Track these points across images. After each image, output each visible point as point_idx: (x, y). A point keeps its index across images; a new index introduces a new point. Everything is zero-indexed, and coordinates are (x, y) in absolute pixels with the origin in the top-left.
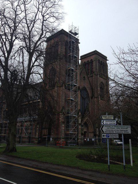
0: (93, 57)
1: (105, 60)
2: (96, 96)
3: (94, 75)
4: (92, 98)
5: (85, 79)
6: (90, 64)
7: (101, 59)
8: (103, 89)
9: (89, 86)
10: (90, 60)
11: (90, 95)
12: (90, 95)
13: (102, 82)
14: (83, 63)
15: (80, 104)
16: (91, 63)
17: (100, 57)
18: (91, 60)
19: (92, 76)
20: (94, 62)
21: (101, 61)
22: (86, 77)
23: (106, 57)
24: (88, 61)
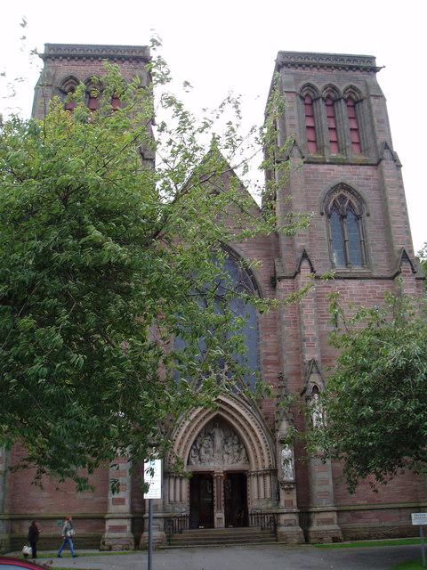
8: (358, 218)
13: (343, 186)
21: (334, 89)
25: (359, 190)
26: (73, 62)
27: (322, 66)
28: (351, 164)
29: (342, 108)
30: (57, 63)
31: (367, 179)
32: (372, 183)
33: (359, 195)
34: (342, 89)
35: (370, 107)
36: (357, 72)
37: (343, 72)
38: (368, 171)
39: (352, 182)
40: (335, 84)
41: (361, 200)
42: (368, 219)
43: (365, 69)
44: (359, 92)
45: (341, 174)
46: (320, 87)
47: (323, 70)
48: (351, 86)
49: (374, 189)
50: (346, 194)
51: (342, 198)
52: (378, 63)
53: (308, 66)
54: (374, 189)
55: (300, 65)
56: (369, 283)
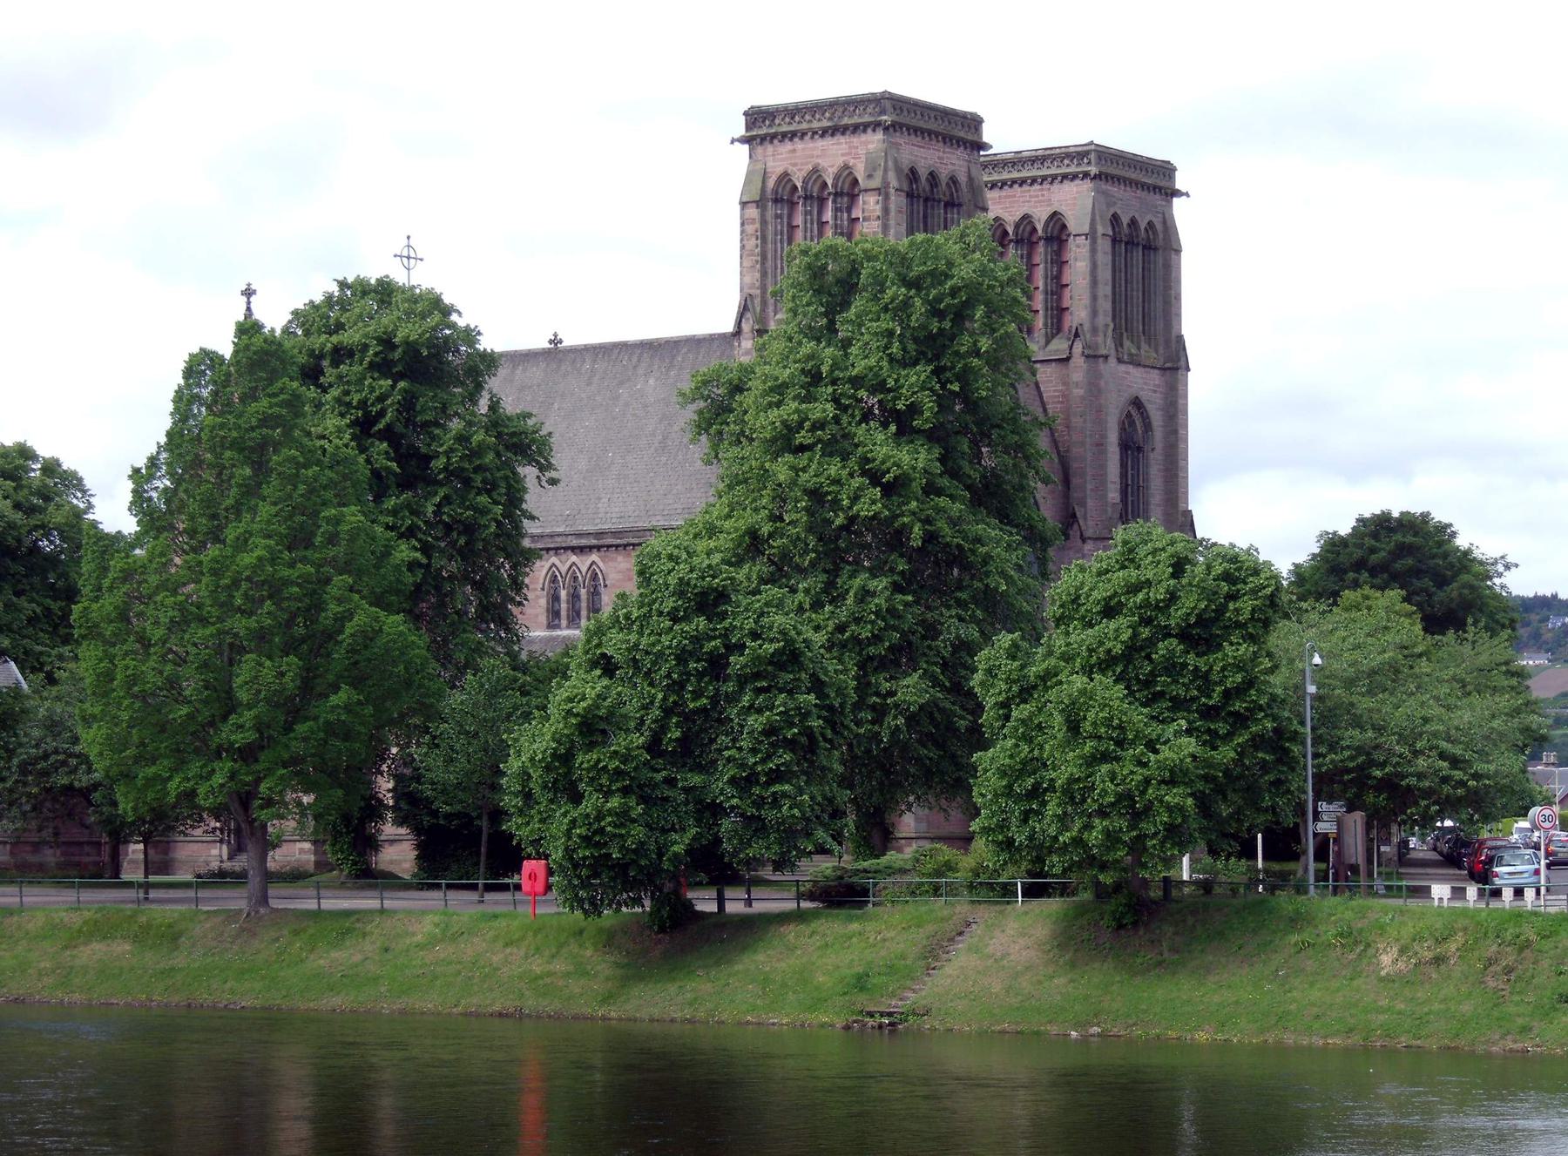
1: (1157, 199)
7: (1129, 204)
8: (1139, 449)
10: (1041, 215)
13: (1137, 403)
18: (1055, 213)
21: (1133, 223)
23: (1165, 170)
24: (1026, 218)
25: (1149, 407)
26: (913, 137)
28: (1145, 366)
29: (1138, 254)
31: (1155, 392)
33: (1148, 417)
36: (1157, 196)
37: (1146, 193)
38: (1155, 376)
39: (1145, 396)
41: (1148, 426)
42: (1151, 456)
46: (1125, 220)
48: (1150, 224)
49: (1158, 409)
52: (1180, 184)
54: (1158, 409)
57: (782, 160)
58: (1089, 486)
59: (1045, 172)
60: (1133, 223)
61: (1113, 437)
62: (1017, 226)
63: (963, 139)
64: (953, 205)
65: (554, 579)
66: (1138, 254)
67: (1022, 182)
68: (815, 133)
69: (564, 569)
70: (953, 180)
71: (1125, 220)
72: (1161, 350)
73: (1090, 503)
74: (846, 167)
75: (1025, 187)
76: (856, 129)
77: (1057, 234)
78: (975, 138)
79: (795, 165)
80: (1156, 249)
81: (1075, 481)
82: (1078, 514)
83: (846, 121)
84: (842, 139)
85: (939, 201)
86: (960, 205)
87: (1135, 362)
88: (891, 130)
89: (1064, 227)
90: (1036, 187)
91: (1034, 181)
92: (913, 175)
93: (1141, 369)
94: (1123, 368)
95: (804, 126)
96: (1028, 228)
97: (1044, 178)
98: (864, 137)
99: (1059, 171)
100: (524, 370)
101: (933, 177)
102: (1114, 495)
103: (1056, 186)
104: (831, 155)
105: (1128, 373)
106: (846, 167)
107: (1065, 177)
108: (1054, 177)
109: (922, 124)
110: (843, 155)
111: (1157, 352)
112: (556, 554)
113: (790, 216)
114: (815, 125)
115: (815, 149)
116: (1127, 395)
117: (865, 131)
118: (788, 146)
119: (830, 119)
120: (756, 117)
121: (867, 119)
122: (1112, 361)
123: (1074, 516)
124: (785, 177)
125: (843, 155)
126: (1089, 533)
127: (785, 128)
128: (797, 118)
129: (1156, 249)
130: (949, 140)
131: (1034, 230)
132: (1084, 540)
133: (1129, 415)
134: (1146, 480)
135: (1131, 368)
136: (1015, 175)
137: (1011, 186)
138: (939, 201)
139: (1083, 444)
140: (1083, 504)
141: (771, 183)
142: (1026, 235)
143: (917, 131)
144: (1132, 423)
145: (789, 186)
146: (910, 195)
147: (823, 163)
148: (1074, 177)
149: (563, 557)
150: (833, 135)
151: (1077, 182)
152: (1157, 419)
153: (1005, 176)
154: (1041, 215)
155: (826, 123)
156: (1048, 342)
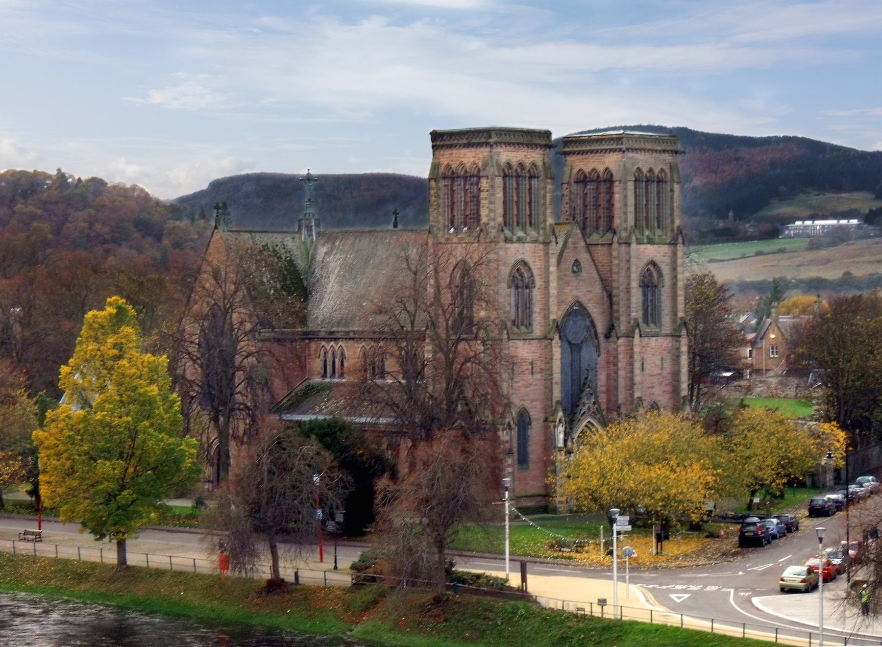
0: (611, 161)
2: (623, 328)
3: (615, 246)
4: (607, 336)
5: (580, 270)
6: (603, 188)
8: (656, 286)
9: (597, 288)
11: (600, 328)
12: (600, 328)
13: (653, 263)
14: (575, 171)
15: (559, 381)
16: (605, 181)
17: (639, 156)
18: (607, 169)
19: (610, 245)
20: (617, 188)
21: (651, 170)
22: (584, 257)
24: (593, 170)
26: (508, 147)
27: (649, 150)
29: (653, 188)
30: (498, 149)
31: (665, 256)
32: (667, 260)
34: (657, 171)
35: (672, 191)
36: (667, 155)
37: (658, 155)
38: (665, 249)
39: (658, 259)
40: (653, 167)
41: (660, 274)
42: (663, 290)
43: (672, 151)
44: (665, 174)
45: (651, 252)
46: (645, 170)
47: (647, 154)
49: (667, 265)
50: (652, 268)
51: (648, 270)
53: (640, 150)
54: (667, 265)
55: (636, 149)
56: (660, 339)
57: (447, 158)
58: (622, 310)
59: (602, 147)
60: (651, 170)
61: (634, 284)
62: (590, 174)
63: (539, 144)
64: (535, 177)
65: (364, 354)
66: (653, 188)
67: (592, 152)
68: (460, 146)
69: (368, 348)
70: (534, 165)
71: (645, 170)
72: (669, 234)
73: (622, 318)
74: (474, 163)
75: (593, 155)
76: (479, 145)
77: (609, 180)
78: (547, 142)
79: (452, 161)
80: (666, 182)
81: (615, 307)
82: (615, 325)
83: (474, 141)
84: (473, 149)
85: (525, 177)
86: (538, 177)
87: (651, 242)
88: (495, 146)
89: (612, 175)
90: (598, 154)
91: (597, 151)
92: (509, 165)
93: (655, 246)
94: (643, 247)
95: (456, 142)
96: (596, 175)
97: (602, 151)
98: (482, 149)
99: (608, 147)
100: (360, 241)
101: (521, 165)
102: (637, 313)
103: (607, 155)
104: (469, 158)
105: (647, 249)
106: (474, 163)
107: (611, 150)
108: (606, 150)
109: (514, 141)
110: (474, 157)
111: (666, 235)
112: (364, 341)
113: (452, 185)
114: (461, 142)
115: (461, 153)
116: (645, 260)
117: (482, 146)
118: (450, 151)
119: (467, 139)
120: (436, 136)
121: (483, 140)
122: (634, 246)
123: (613, 325)
124: (448, 166)
125: (474, 157)
126: (619, 335)
127: (447, 143)
128: (453, 138)
129: (666, 182)
130: (530, 145)
131: (598, 176)
132: (618, 338)
133: (648, 270)
134: (659, 302)
135: (648, 246)
136: (588, 148)
137: (587, 153)
138: (525, 177)
139: (618, 288)
140: (618, 319)
141: (442, 170)
142: (595, 178)
143: (510, 144)
144: (651, 275)
145: (451, 171)
146: (505, 176)
147: (465, 161)
148: (614, 150)
149: (368, 343)
150: (468, 147)
151: (617, 153)
152: (666, 270)
153: (584, 148)
154: (601, 168)
155: (465, 141)
156: (604, 235)
